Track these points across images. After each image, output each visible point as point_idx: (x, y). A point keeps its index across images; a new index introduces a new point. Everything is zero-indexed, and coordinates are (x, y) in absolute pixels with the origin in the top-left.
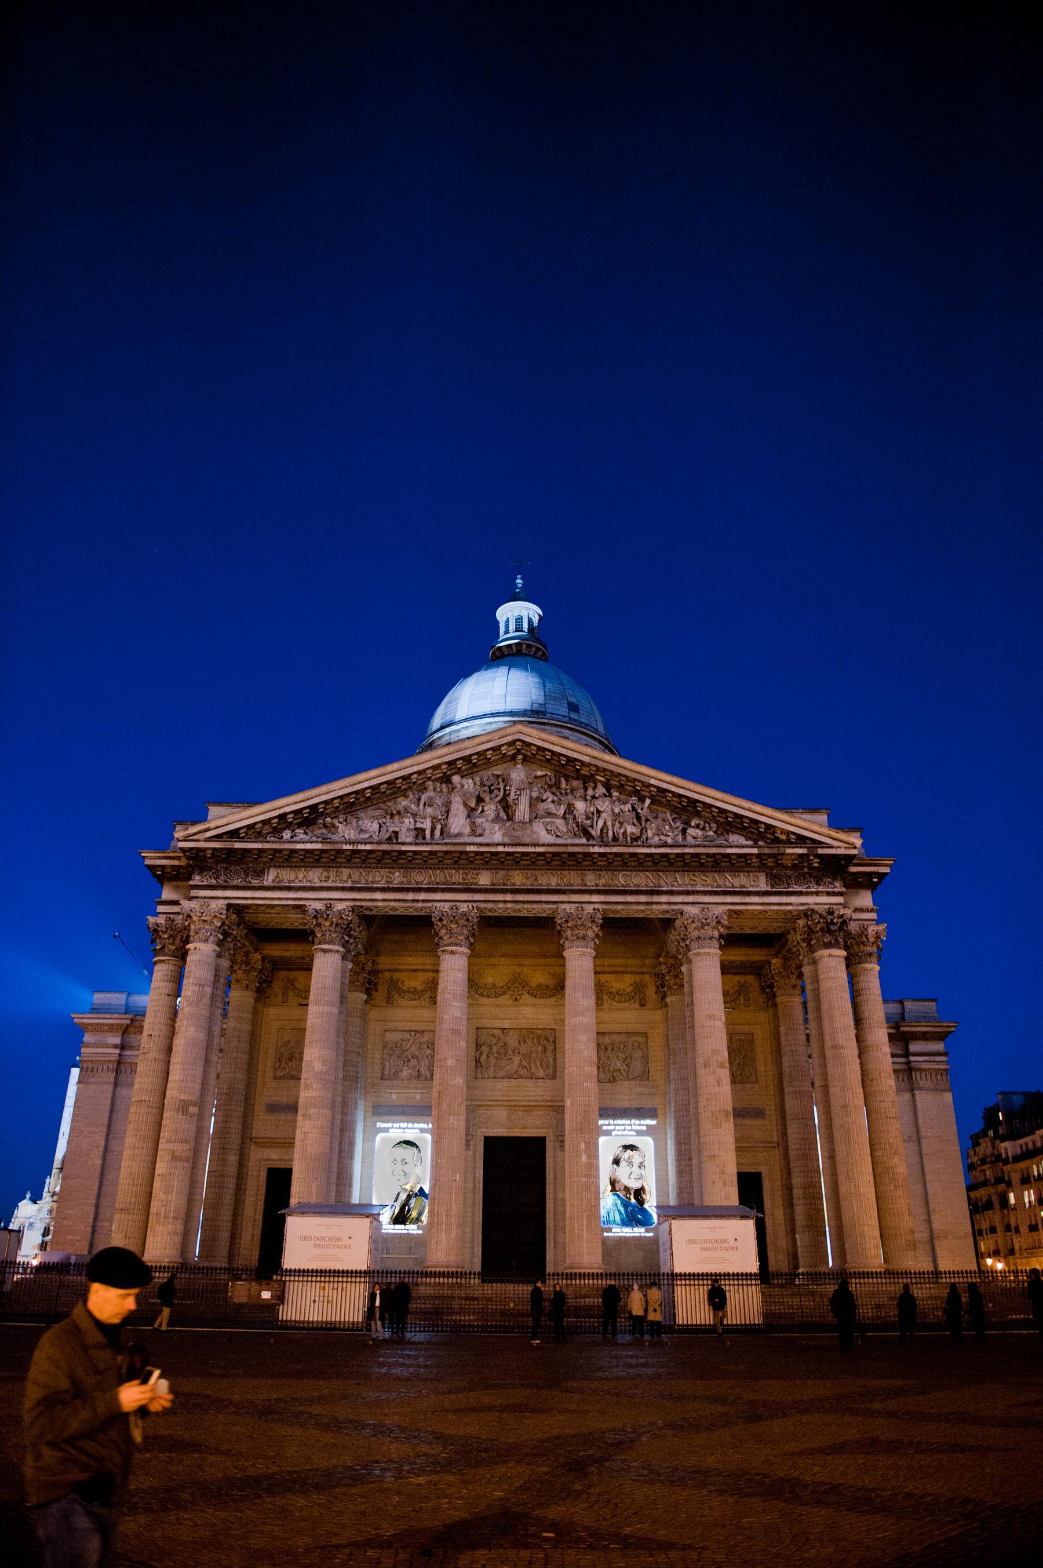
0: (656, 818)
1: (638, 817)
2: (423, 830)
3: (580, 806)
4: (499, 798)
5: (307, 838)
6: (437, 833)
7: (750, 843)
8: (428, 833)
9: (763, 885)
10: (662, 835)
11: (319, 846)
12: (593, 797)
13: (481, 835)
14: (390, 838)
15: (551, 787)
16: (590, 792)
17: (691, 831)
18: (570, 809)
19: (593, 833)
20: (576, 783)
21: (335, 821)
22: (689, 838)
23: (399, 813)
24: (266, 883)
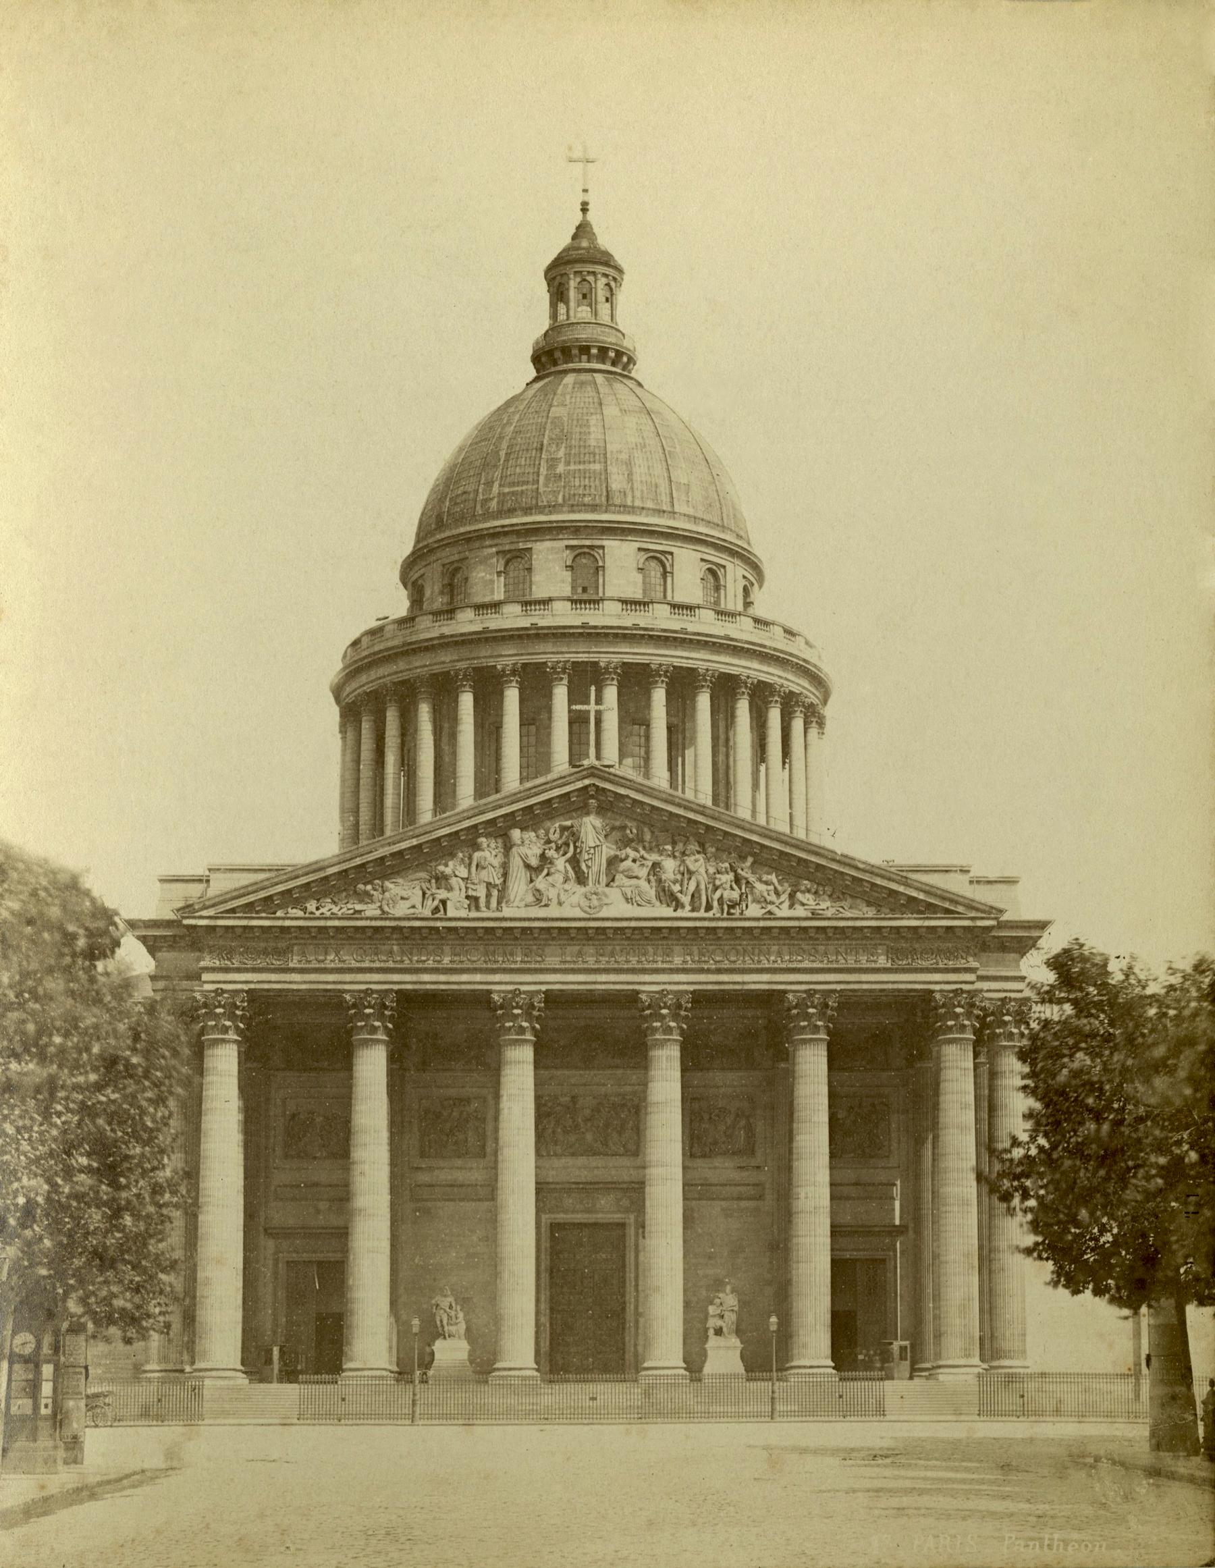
0: (760, 880)
2: (476, 899)
3: (670, 866)
4: (569, 855)
5: (335, 909)
7: (871, 912)
8: (482, 901)
9: (882, 961)
12: (683, 854)
13: (546, 905)
14: (436, 910)
15: (632, 840)
16: (680, 847)
17: (799, 895)
21: (369, 887)
22: (797, 906)
23: (446, 878)
24: (291, 965)
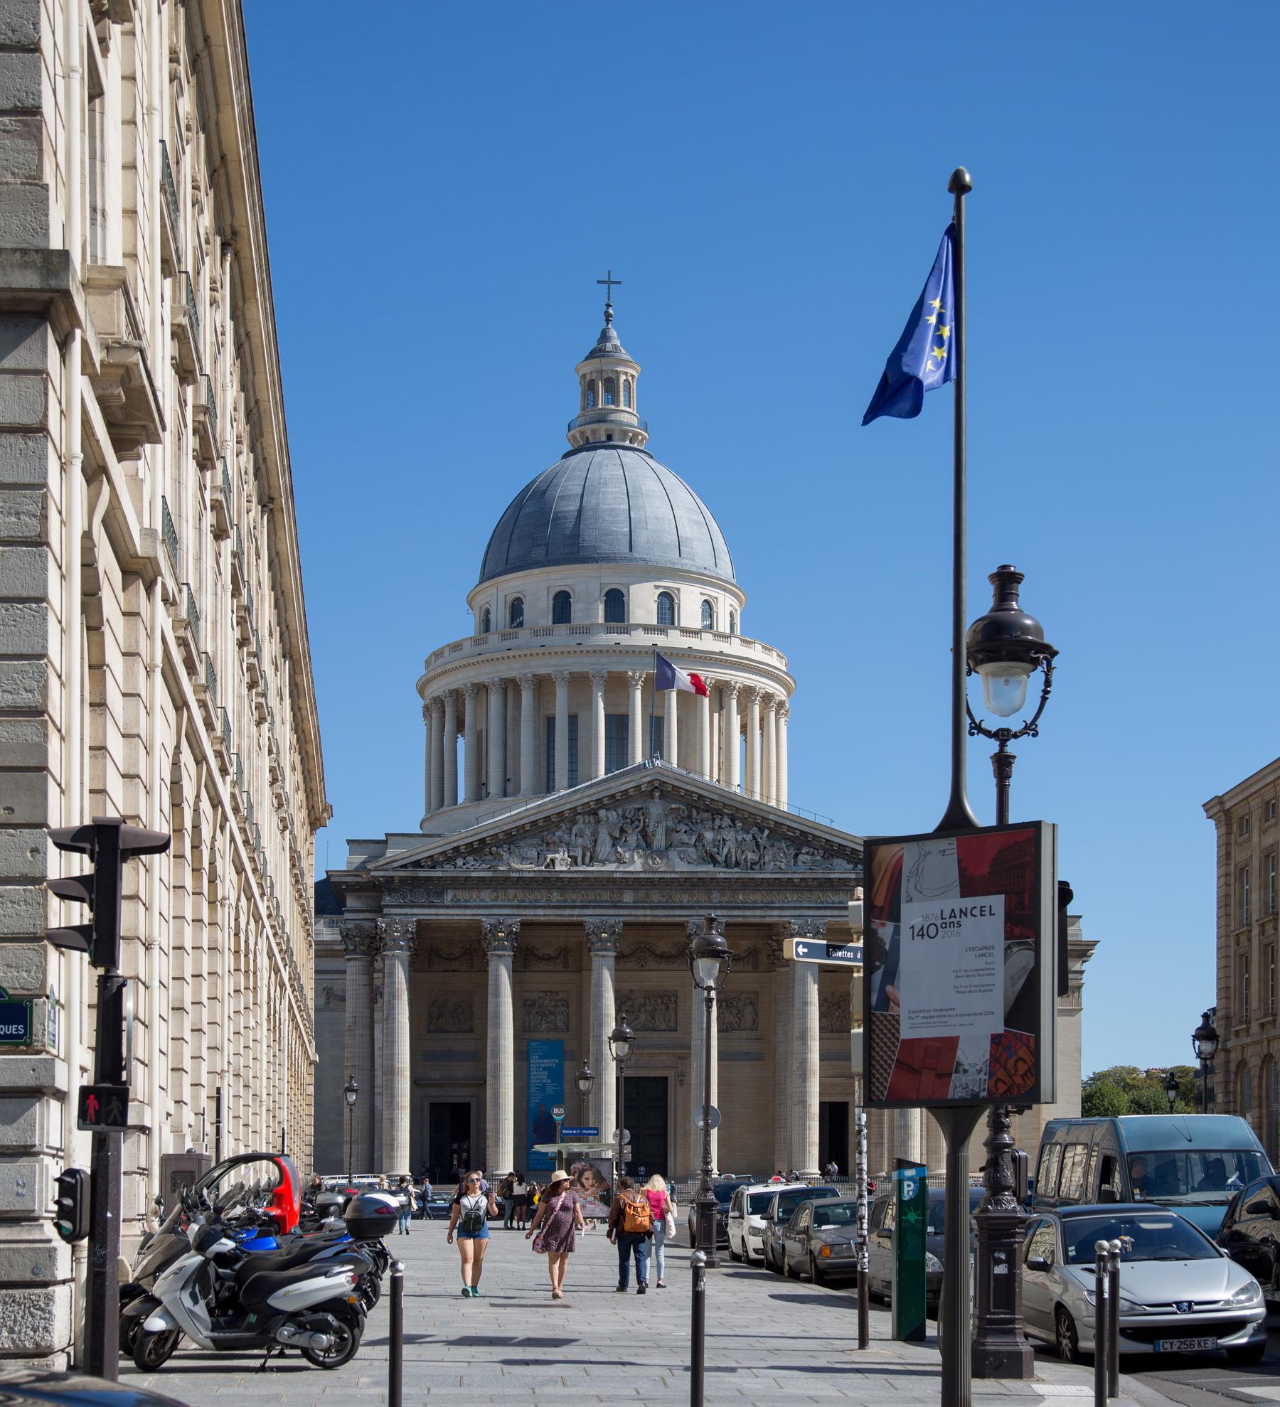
0: (773, 846)
1: (758, 845)
3: (709, 835)
6: (587, 859)
7: (851, 866)
8: (579, 859)
10: (777, 864)
11: (490, 874)
12: (720, 827)
16: (717, 822)
17: (800, 857)
18: (700, 838)
19: (719, 859)
20: (706, 815)
21: (500, 851)
22: (799, 863)
23: (554, 843)
24: (446, 903)
